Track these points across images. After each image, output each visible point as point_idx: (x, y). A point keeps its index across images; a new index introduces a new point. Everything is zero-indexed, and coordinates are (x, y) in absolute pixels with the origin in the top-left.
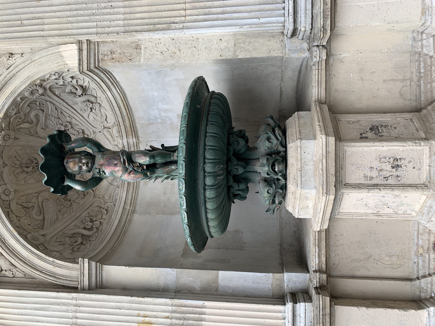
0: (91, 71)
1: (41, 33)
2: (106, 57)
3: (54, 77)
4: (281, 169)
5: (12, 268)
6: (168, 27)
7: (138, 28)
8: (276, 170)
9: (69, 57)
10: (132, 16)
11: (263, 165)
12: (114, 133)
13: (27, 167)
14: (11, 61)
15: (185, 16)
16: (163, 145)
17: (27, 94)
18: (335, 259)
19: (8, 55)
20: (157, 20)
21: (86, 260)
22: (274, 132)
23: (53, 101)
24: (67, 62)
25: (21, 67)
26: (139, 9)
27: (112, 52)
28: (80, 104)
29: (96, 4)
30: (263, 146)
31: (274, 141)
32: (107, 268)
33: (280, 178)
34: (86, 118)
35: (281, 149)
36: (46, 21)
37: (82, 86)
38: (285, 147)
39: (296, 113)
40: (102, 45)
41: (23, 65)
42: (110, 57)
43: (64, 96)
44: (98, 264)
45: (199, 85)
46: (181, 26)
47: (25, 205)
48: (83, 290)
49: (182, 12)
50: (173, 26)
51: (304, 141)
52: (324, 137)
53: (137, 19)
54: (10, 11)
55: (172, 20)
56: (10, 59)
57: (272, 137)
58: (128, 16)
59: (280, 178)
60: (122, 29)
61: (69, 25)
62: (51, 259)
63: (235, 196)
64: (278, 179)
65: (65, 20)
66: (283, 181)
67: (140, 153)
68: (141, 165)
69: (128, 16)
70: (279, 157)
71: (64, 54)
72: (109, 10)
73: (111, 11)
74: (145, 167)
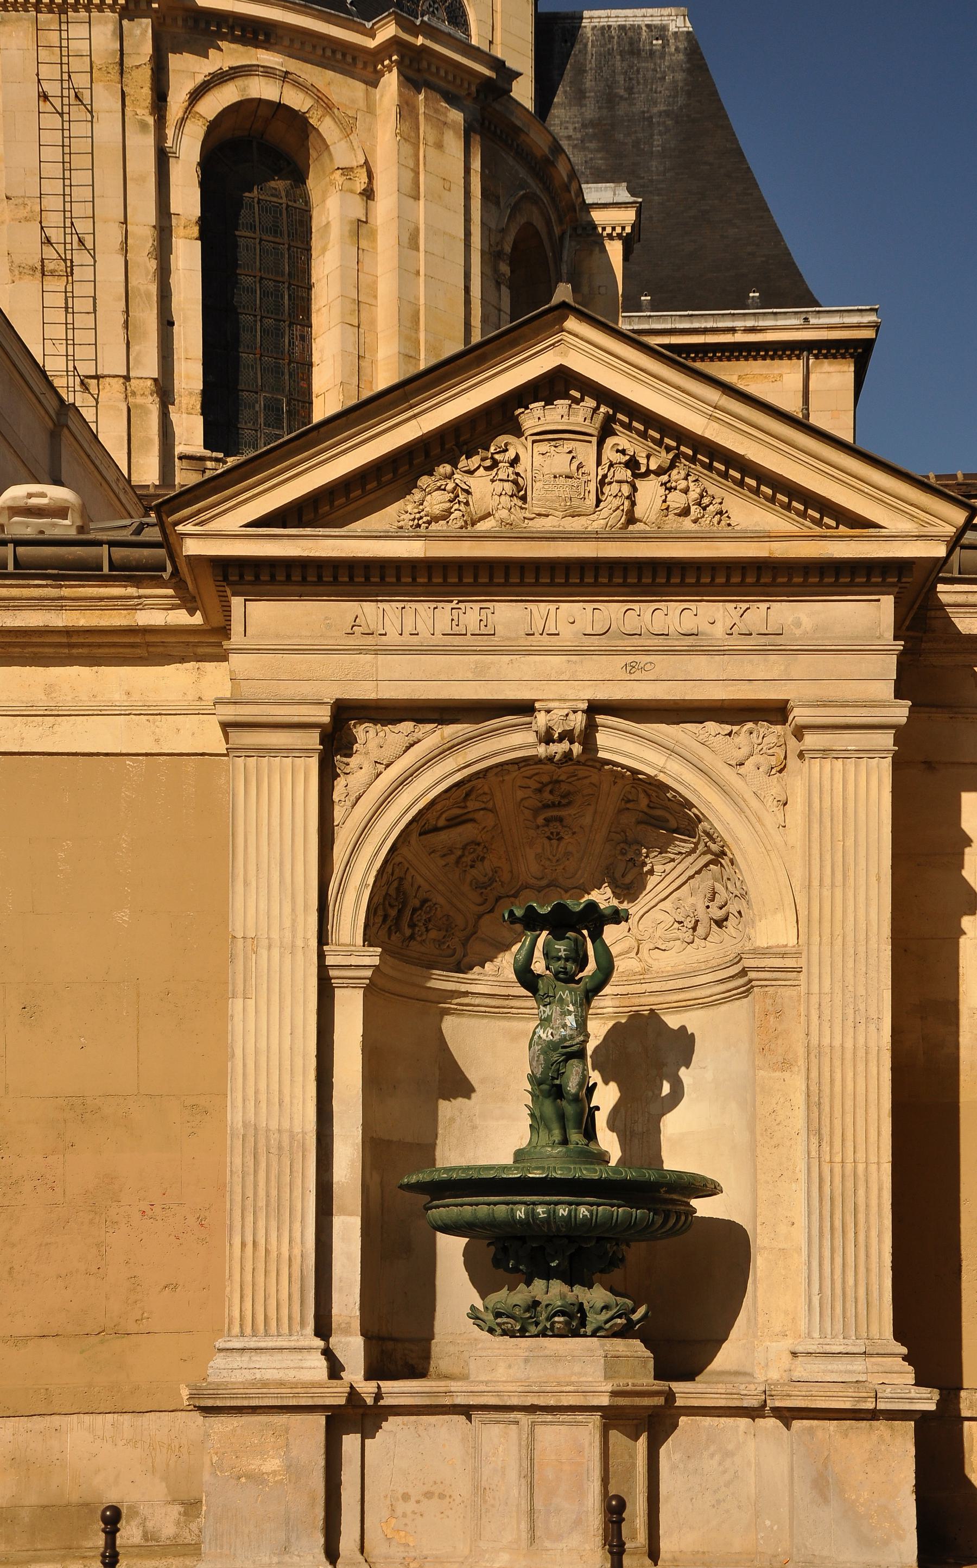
0: (744, 972)
1: (816, 883)
2: (771, 1001)
3: (738, 884)
4: (557, 1325)
5: (353, 798)
6: (815, 1129)
7: (814, 1074)
8: (556, 1319)
9: (773, 930)
10: (837, 1063)
11: (563, 1297)
12: (627, 960)
13: (551, 792)
14: (769, 801)
15: (831, 1162)
16: (597, 1108)
17: (704, 825)
18: (392, 1424)
19: (783, 799)
20: (826, 1109)
21: (376, 961)
22: (620, 1317)
23: (694, 856)
24: (763, 921)
25: (757, 826)
26: (850, 1075)
27: (779, 1013)
28: (691, 900)
29: (864, 993)
30: (595, 1297)
31: (605, 1316)
32: (358, 995)
33: (540, 1328)
34: (660, 906)
35: (589, 1330)
36: (838, 893)
37: (726, 919)
38: (594, 1335)
39: (649, 1354)
40: (795, 993)
41: (761, 832)
42: (771, 1008)
43: (704, 882)
44: (368, 981)
45: (707, 1188)
46: (814, 1154)
47: (473, 796)
48: (321, 956)
49: (838, 1158)
50: (814, 1140)
51: (602, 1361)
52: (609, 1388)
53: (832, 1072)
54: (862, 816)
55: (826, 1138)
56: (775, 802)
57: (610, 1314)
58: (838, 1054)
59: (540, 1328)
60: (814, 1042)
61: (826, 938)
62: (371, 881)
63: (505, 1250)
64: (537, 1324)
65: (838, 931)
66: (533, 1330)
67: (583, 1073)
68: (560, 1075)
69: (838, 1054)
70: (574, 1323)
71: (779, 916)
72: (851, 1019)
73: (850, 1023)
74: (557, 1082)
